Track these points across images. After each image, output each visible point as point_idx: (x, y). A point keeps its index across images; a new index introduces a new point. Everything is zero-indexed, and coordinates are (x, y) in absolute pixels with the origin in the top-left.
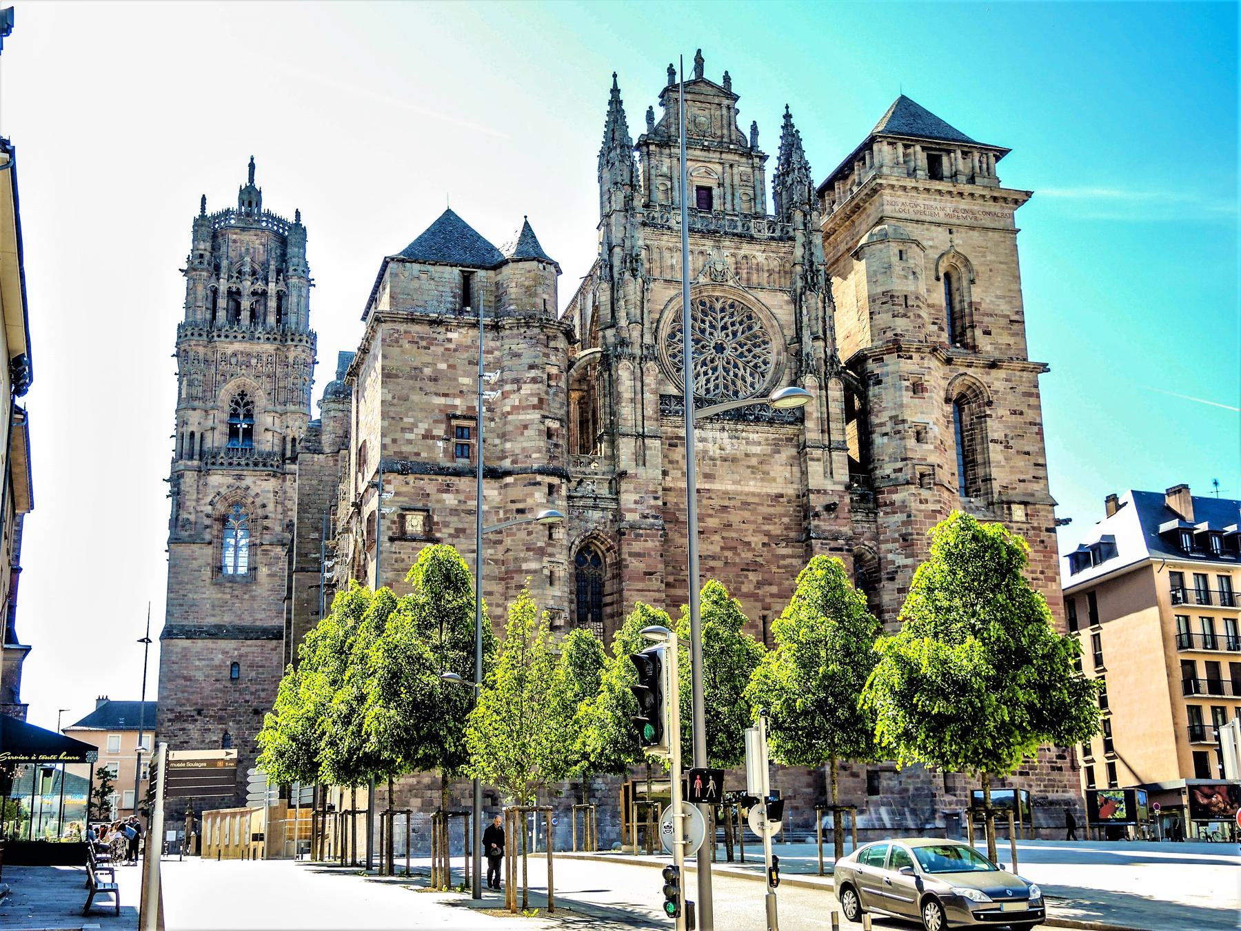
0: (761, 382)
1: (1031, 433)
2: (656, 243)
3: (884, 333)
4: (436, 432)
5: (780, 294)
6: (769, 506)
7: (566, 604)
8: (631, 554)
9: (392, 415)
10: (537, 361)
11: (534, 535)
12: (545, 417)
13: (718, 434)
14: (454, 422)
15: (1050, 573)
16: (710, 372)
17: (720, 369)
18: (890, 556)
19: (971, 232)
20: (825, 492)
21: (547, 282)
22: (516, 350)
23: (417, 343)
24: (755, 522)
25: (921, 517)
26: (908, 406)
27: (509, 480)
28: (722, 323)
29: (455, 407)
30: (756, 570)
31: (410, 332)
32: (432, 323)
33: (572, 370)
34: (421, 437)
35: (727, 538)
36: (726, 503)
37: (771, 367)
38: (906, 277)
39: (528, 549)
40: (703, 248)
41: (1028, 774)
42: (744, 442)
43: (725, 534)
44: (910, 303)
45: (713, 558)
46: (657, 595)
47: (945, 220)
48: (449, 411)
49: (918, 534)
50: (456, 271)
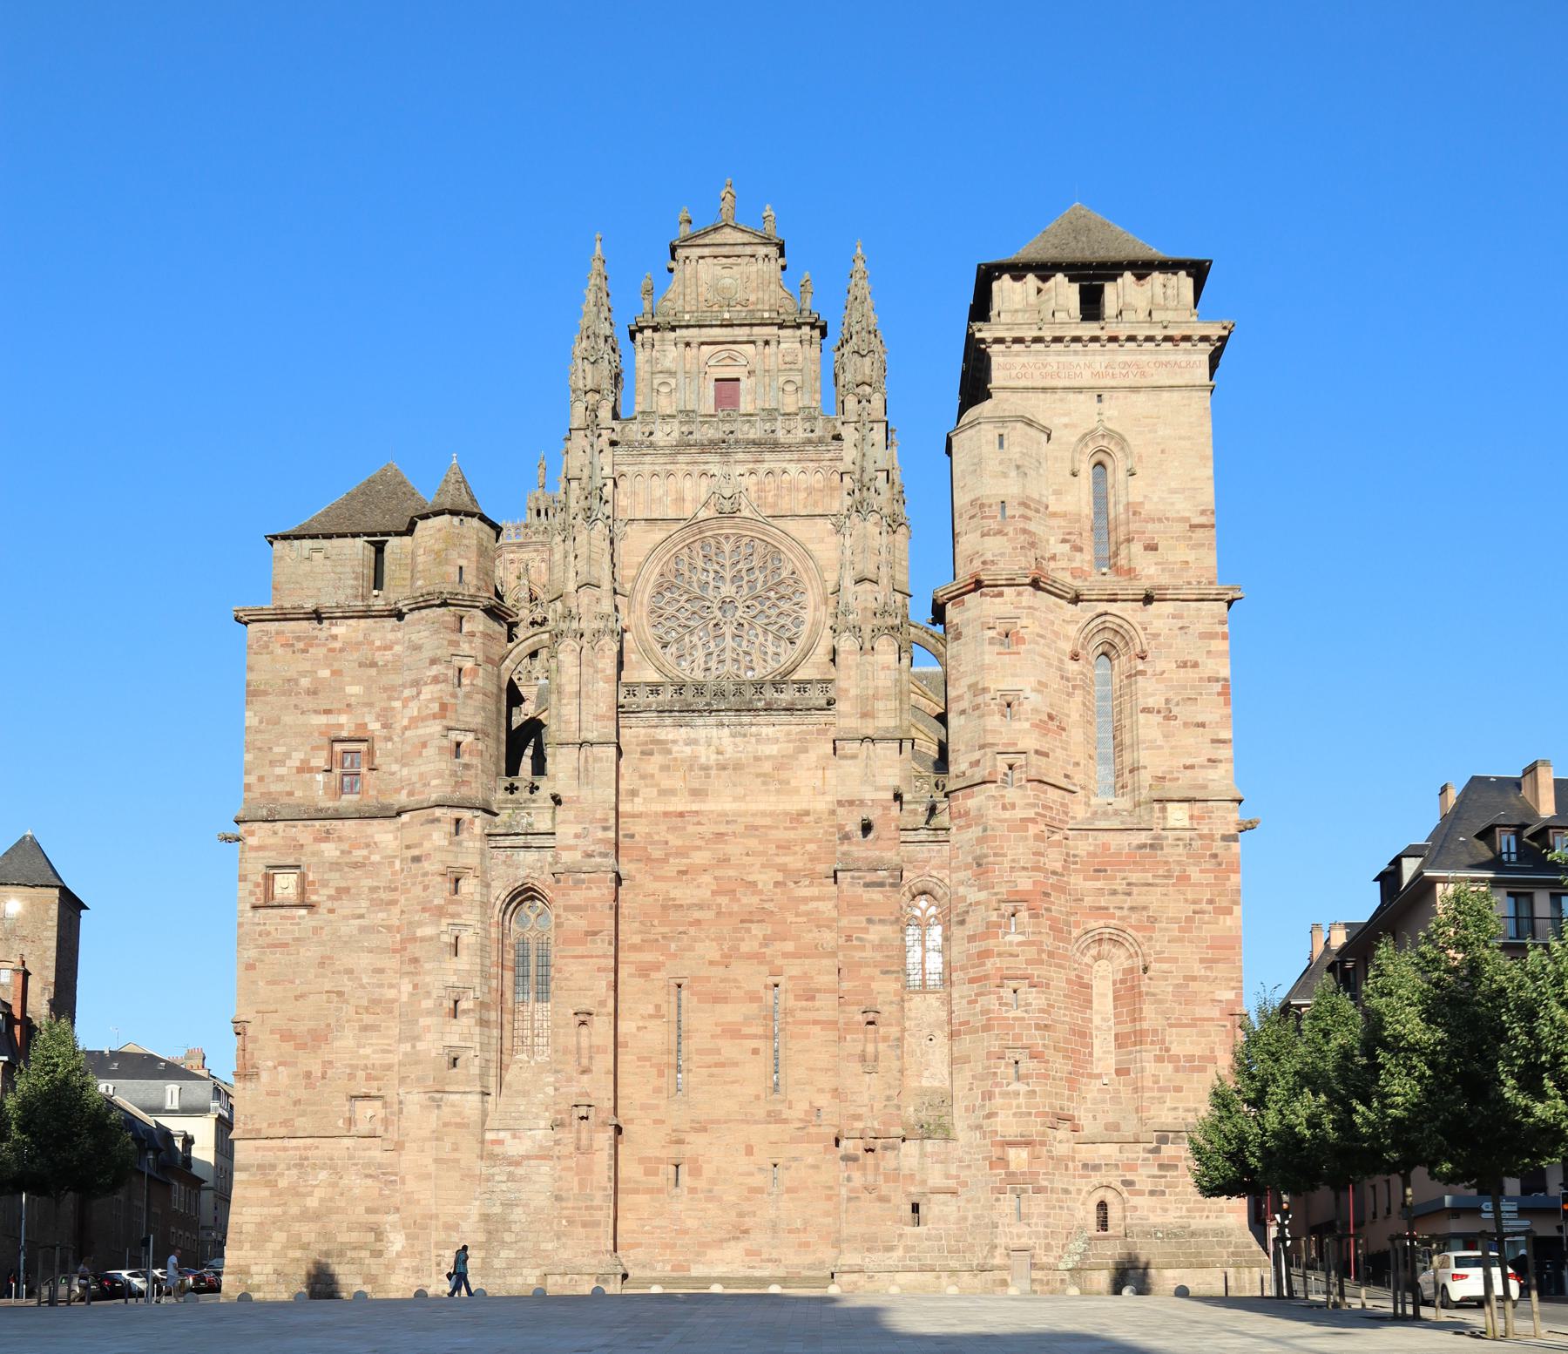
0: (789, 651)
1: (1210, 694)
2: (636, 468)
3: (971, 561)
4: (315, 763)
5: (820, 521)
6: (785, 828)
7: (477, 980)
8: (566, 908)
9: (258, 744)
11: (431, 890)
12: (449, 729)
13: (714, 732)
14: (338, 747)
15: (1223, 902)
16: (712, 644)
18: (962, 890)
19: (1134, 396)
20: (862, 803)
21: (466, 542)
24: (764, 853)
27: (405, 817)
29: (341, 726)
30: (763, 921)
31: (283, 632)
32: (317, 616)
33: (508, 661)
34: (294, 770)
36: (723, 828)
39: (424, 910)
41: (1163, 1193)
42: (753, 740)
43: (719, 873)
45: (700, 907)
47: (1092, 383)
48: (334, 734)
49: (996, 855)
50: (360, 541)
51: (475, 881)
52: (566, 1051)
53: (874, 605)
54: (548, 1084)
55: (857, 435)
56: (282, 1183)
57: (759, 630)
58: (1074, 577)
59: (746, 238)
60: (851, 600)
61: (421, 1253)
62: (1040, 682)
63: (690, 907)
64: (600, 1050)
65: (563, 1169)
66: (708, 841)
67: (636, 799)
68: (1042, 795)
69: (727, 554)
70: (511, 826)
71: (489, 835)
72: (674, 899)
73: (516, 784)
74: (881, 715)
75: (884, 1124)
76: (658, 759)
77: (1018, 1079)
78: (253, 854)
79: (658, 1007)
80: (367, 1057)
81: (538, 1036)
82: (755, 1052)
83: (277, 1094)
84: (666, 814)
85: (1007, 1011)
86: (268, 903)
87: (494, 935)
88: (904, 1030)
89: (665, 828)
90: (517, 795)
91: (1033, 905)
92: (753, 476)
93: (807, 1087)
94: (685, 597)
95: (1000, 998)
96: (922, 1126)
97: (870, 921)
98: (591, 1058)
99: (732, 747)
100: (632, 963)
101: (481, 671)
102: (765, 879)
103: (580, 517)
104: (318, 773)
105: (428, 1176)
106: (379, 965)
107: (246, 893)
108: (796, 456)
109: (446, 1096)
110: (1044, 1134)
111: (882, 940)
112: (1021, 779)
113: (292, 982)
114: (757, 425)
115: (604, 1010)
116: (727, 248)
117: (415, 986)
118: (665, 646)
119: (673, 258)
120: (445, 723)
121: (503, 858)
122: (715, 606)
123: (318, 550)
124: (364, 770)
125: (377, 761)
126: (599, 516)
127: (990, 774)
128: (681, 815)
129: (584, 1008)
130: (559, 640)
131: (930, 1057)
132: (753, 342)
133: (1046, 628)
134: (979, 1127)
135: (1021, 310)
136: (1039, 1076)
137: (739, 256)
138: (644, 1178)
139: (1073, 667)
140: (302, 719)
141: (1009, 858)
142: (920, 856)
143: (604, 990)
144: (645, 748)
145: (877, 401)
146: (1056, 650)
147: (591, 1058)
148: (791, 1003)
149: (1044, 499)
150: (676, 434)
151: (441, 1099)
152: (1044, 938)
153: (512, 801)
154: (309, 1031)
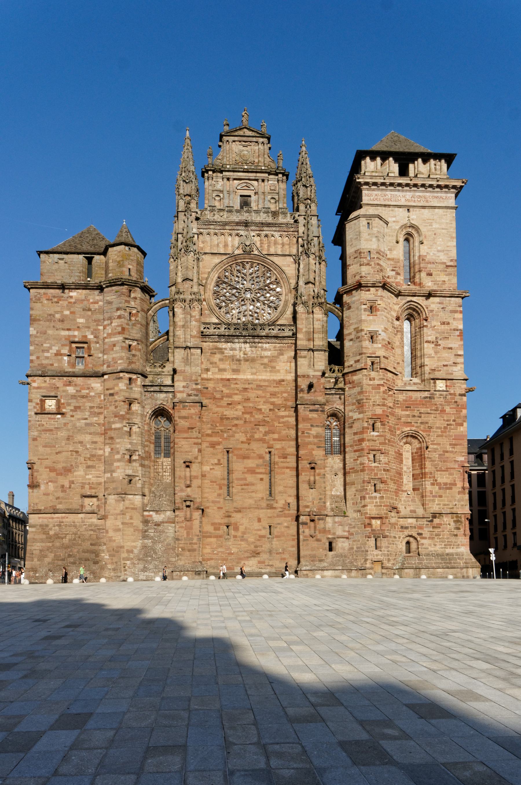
2: (207, 231)
3: (355, 276)
6: (274, 387)
7: (140, 447)
8: (180, 417)
11: (119, 408)
18: (351, 414)
19: (423, 210)
20: (308, 376)
22: (110, 300)
23: (52, 300)
24: (265, 397)
27: (106, 377)
33: (150, 312)
34: (54, 355)
36: (247, 386)
37: (282, 303)
39: (115, 416)
40: (238, 232)
42: (260, 349)
45: (237, 419)
46: (196, 441)
49: (367, 399)
50: (81, 257)
51: (138, 405)
56: (52, 533)
59: (253, 134)
61: (116, 563)
63: (232, 419)
64: (196, 477)
65: (179, 527)
66: (240, 391)
67: (209, 373)
70: (153, 382)
71: (144, 386)
72: (226, 415)
75: (318, 509)
76: (218, 356)
78: (35, 391)
80: (90, 479)
83: (48, 494)
84: (222, 379)
86: (42, 412)
89: (221, 385)
92: (259, 237)
95: (368, 458)
97: (312, 426)
102: (265, 408)
104: (65, 356)
105: (119, 530)
106: (95, 440)
107: (32, 408)
108: (278, 229)
109: (127, 496)
111: (317, 433)
112: (377, 368)
113: (55, 447)
115: (197, 461)
117: (112, 449)
118: (220, 308)
119: (221, 141)
122: (242, 292)
123: (62, 259)
124: (86, 356)
125: (92, 352)
128: (228, 380)
130: (175, 302)
132: (257, 180)
137: (251, 142)
138: (214, 531)
139: (397, 323)
140: (57, 332)
143: (197, 452)
144: (212, 351)
146: (391, 315)
147: (191, 481)
149: (386, 252)
151: (125, 497)
152: (386, 434)
154: (63, 467)
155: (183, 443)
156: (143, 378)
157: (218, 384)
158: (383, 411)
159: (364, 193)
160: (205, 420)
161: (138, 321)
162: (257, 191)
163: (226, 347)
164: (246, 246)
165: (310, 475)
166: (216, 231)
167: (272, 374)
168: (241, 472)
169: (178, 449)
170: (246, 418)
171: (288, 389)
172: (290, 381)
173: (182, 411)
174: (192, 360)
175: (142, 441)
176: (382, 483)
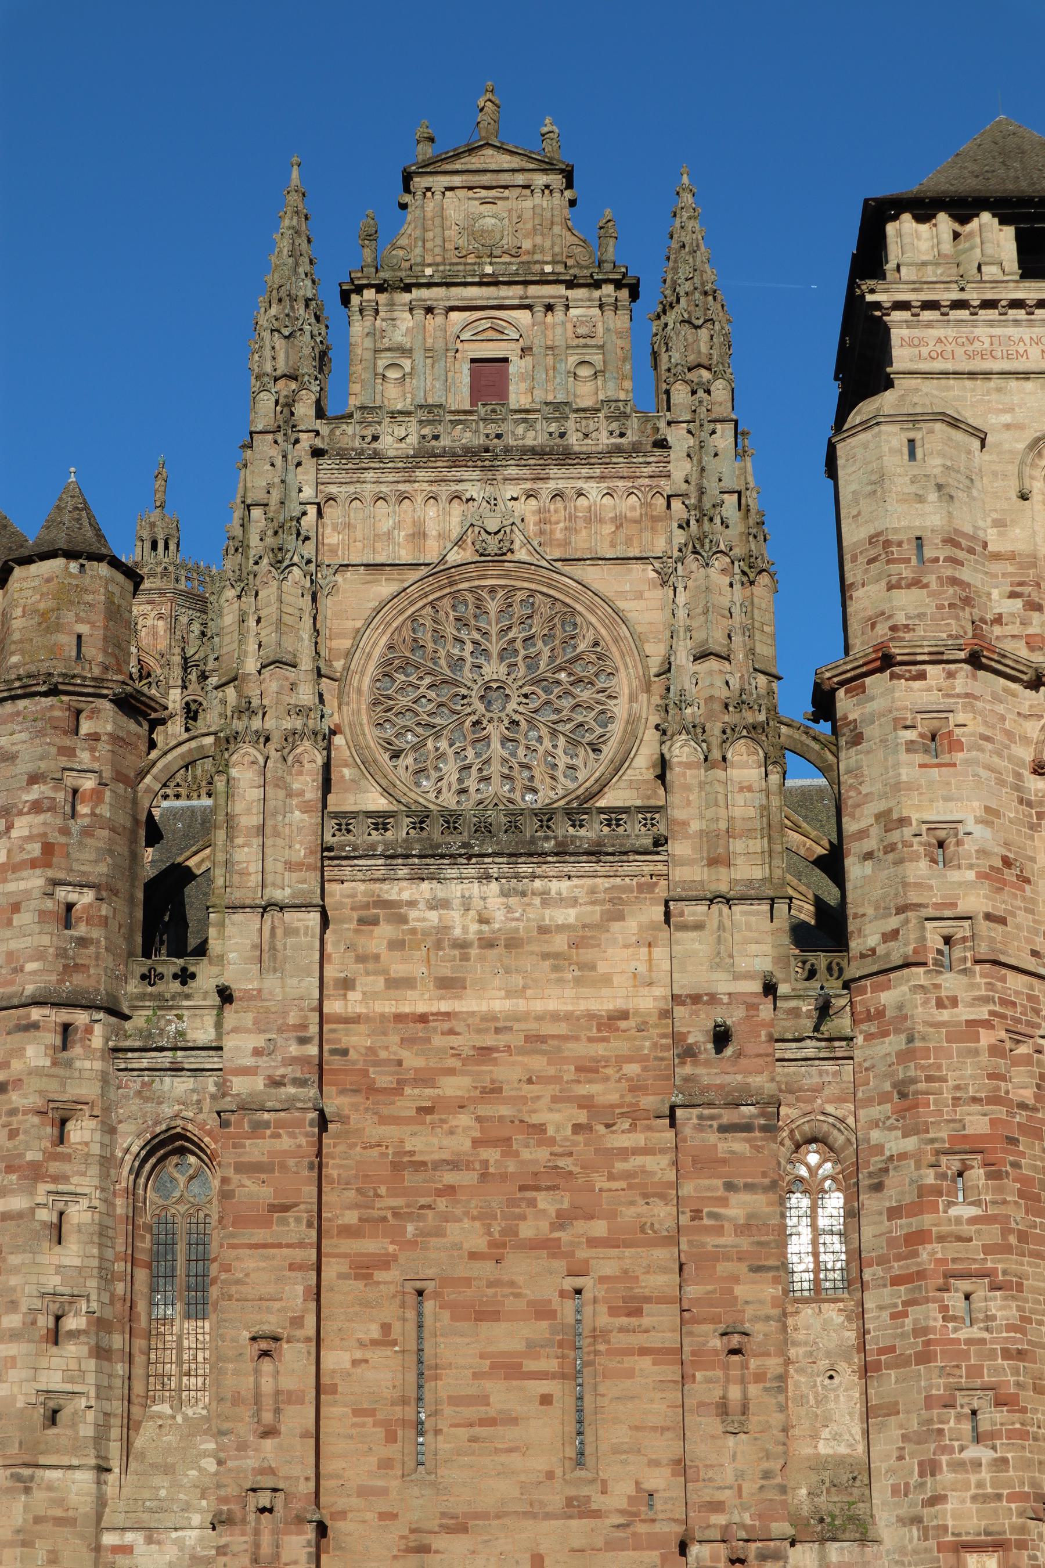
0: (591, 763)
2: (351, 489)
3: (873, 626)
5: (636, 567)
6: (590, 1040)
7: (92, 1283)
8: (240, 1168)
10: (43, 765)
11: (21, 1137)
12: (56, 883)
16: (470, 753)
17: (495, 743)
18: (875, 1136)
20: (713, 999)
21: (89, 598)
24: (556, 1079)
25: (938, 1039)
26: (911, 786)
28: (503, 643)
30: (555, 1188)
33: (148, 779)
35: (488, 1119)
36: (489, 1040)
37: (616, 729)
38: (920, 499)
39: (10, 1169)
40: (460, 487)
42: (537, 901)
43: (484, 1110)
44: (929, 553)
45: (454, 1165)
49: (929, 1079)
51: (93, 1124)
52: (237, 1400)
53: (725, 693)
54: (206, 1454)
55: (691, 441)
57: (544, 731)
58: (1032, 649)
59: (515, 162)
60: (688, 684)
62: (987, 809)
63: (437, 1165)
64: (294, 1398)
67: (351, 995)
68: (999, 984)
69: (493, 615)
70: (150, 1035)
71: (116, 1050)
72: (412, 1153)
73: (159, 970)
74: (740, 861)
75: (760, 1516)
76: (385, 931)
77: (978, 1438)
79: (386, 1328)
81: (188, 1374)
82: (546, 1400)
84: (399, 1018)
85: (956, 1330)
87: (120, 1211)
88: (788, 1362)
89: (396, 1039)
90: (160, 987)
91: (991, 1158)
92: (532, 501)
93: (632, 1458)
94: (428, 680)
95: (944, 1308)
96: (822, 1521)
97: (730, 1187)
98: (277, 1411)
99: (503, 911)
100: (345, 1256)
101: (108, 794)
103: (265, 561)
108: (598, 471)
109: (39, 1473)
110: (1023, 1529)
111: (750, 1216)
114: (538, 426)
115: (300, 1333)
116: (489, 176)
118: (395, 756)
119: (407, 190)
120: (50, 873)
121: (137, 1086)
126: (296, 559)
127: (916, 951)
128: (423, 1018)
129: (267, 1328)
131: (832, 1405)
132: (529, 307)
133: (993, 727)
134: (917, 1520)
135: (931, 263)
136: (1011, 1434)
137: (506, 187)
141: (951, 1083)
142: (807, 1082)
143: (300, 1301)
144: (364, 913)
145: (720, 390)
146: (1011, 759)
147: (277, 1411)
148: (604, 1320)
149: (981, 534)
150: (413, 440)
151: (32, 1478)
152: (1010, 1210)
153: (152, 997)
155: (250, 1264)
156: (113, 1020)
157: (385, 1034)
158: (993, 1122)
159: (897, 334)
160: (334, 1173)
161: (101, 816)
162: (528, 343)
163: (416, 897)
164: (489, 533)
165: (727, 1380)
166: (384, 488)
167: (585, 991)
168: (468, 1373)
169: (233, 1289)
170: (485, 1163)
171: (642, 1048)
172: (649, 1014)
173: (248, 1142)
174: (288, 953)
175: (101, 1258)
176: (997, 1405)
